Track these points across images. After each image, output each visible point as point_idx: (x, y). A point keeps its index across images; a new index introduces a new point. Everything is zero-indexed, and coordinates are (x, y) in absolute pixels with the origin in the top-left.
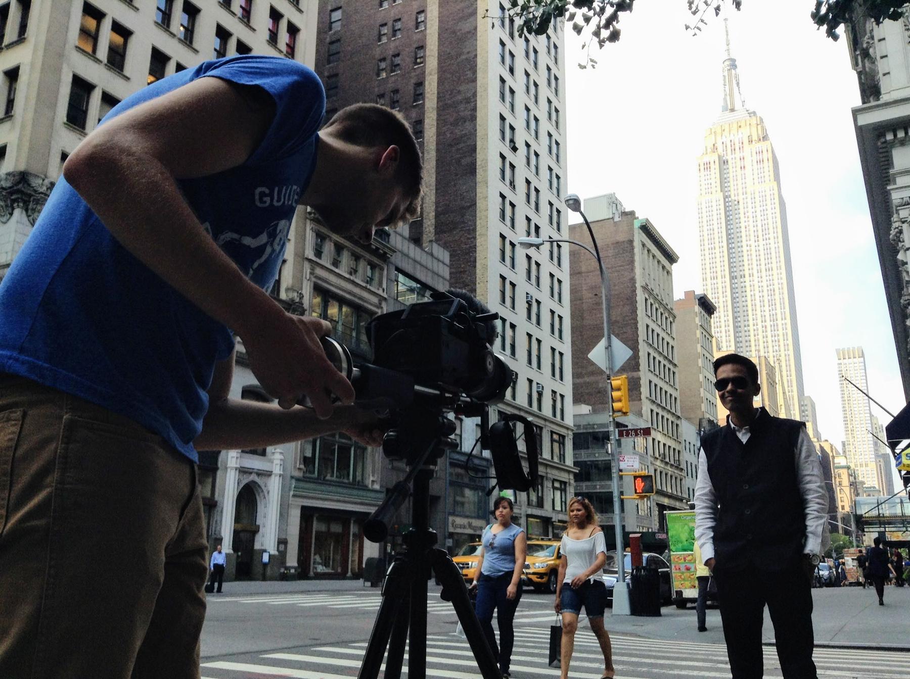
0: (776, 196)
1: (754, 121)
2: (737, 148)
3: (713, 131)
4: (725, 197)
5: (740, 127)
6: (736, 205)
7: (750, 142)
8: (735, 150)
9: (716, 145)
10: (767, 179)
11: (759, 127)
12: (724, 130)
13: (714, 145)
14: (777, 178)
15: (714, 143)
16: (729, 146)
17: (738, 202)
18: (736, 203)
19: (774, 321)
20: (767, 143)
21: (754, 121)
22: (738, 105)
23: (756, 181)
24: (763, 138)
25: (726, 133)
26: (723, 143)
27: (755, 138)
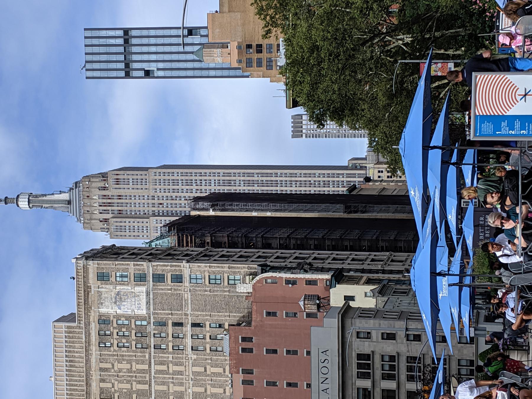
0: (159, 170)
2: (109, 201)
3: (86, 221)
4: (154, 215)
5: (88, 197)
6: (163, 207)
7: (105, 188)
8: (110, 203)
9: (101, 219)
10: (143, 177)
12: (88, 211)
13: (101, 221)
14: (146, 169)
16: (105, 208)
17: (161, 204)
18: (161, 206)
19: (278, 184)
22: (65, 196)
23: (144, 186)
24: (103, 177)
26: (101, 213)
27: (102, 184)
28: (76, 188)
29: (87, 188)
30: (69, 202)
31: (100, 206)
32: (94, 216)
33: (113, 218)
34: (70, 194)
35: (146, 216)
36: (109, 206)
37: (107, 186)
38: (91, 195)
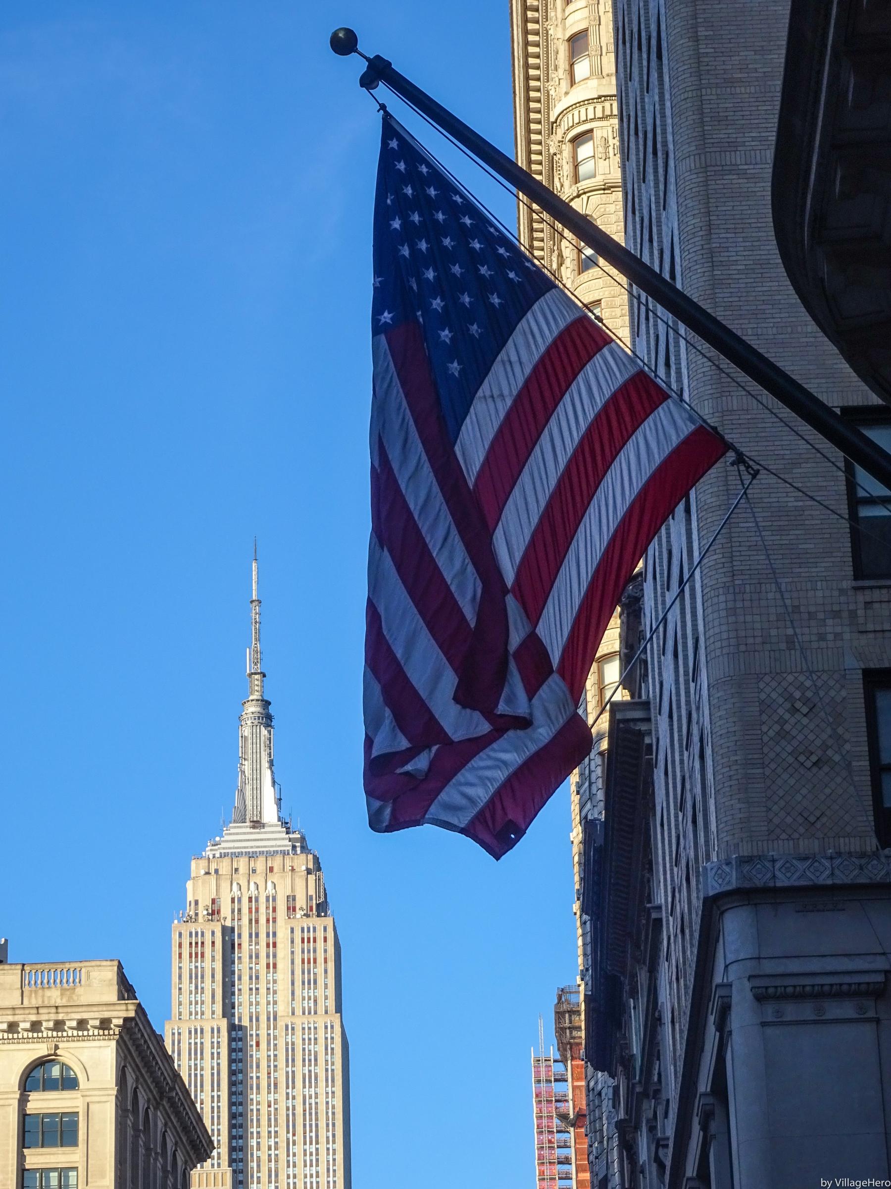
1: (302, 862)
5: (271, 869)
7: (291, 909)
11: (311, 878)
12: (236, 870)
13: (213, 901)
20: (329, 921)
21: (302, 862)
27: (301, 902)
28: (290, 840)
29: (292, 867)
30: (257, 824)
31: (250, 899)
32: (225, 885)
33: (224, 928)
34: (276, 826)
35: (228, 1009)
36: (250, 921)
37: (298, 916)
38: (275, 878)
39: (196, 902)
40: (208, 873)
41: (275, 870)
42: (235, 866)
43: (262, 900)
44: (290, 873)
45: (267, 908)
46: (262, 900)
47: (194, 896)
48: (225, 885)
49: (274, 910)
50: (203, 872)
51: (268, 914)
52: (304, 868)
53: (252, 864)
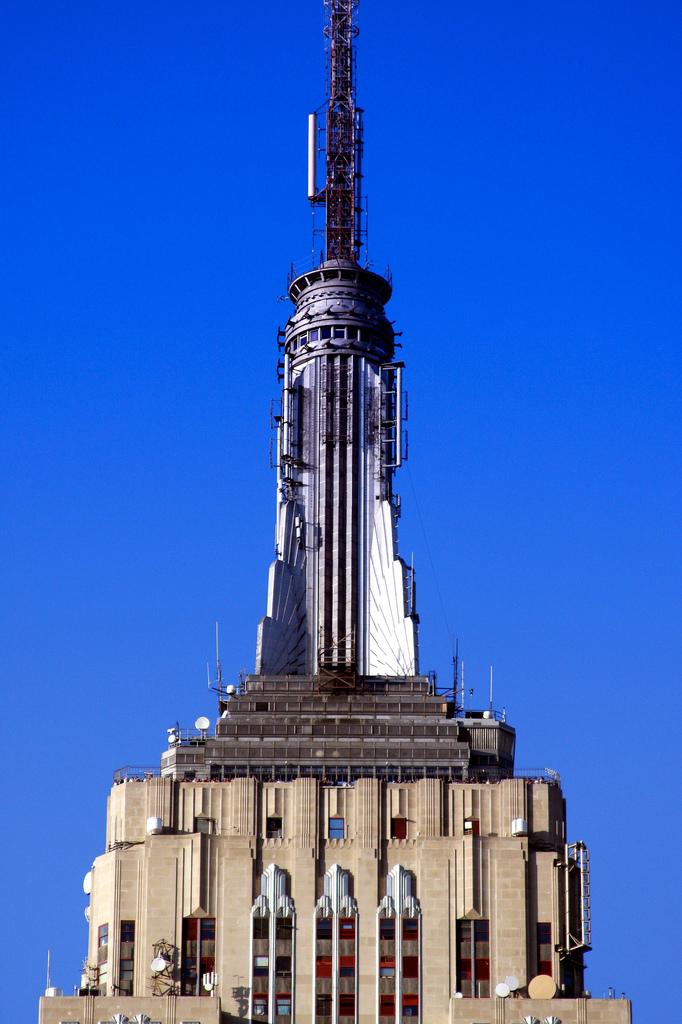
5: (400, 828)
12: (275, 825)
15: (191, 906)
25: (292, 852)
26: (260, 928)
32: (233, 873)
39: (127, 931)
40: (170, 830)
41: (415, 830)
42: (270, 809)
43: (369, 930)
44: (469, 839)
45: (386, 961)
46: (369, 930)
47: (119, 904)
48: (233, 873)
49: (411, 967)
50: (152, 824)
51: (386, 983)
52: (518, 826)
53: (331, 809)
